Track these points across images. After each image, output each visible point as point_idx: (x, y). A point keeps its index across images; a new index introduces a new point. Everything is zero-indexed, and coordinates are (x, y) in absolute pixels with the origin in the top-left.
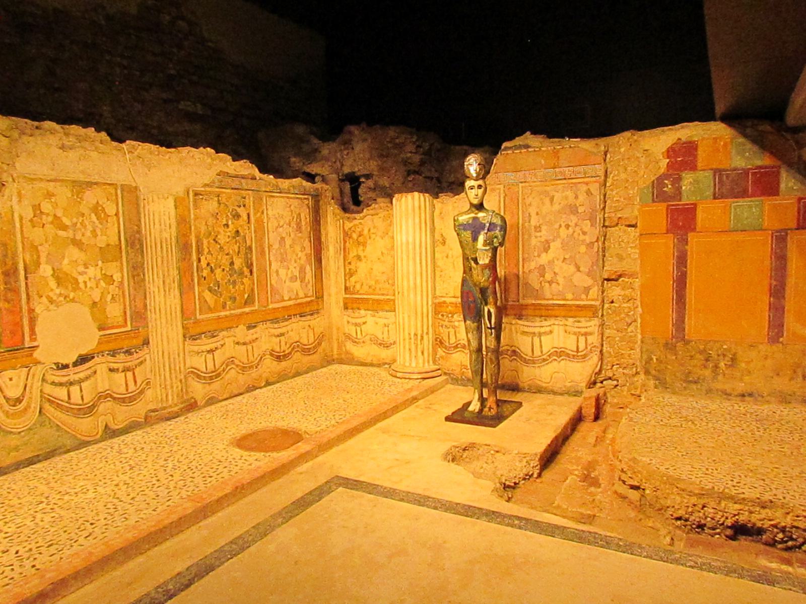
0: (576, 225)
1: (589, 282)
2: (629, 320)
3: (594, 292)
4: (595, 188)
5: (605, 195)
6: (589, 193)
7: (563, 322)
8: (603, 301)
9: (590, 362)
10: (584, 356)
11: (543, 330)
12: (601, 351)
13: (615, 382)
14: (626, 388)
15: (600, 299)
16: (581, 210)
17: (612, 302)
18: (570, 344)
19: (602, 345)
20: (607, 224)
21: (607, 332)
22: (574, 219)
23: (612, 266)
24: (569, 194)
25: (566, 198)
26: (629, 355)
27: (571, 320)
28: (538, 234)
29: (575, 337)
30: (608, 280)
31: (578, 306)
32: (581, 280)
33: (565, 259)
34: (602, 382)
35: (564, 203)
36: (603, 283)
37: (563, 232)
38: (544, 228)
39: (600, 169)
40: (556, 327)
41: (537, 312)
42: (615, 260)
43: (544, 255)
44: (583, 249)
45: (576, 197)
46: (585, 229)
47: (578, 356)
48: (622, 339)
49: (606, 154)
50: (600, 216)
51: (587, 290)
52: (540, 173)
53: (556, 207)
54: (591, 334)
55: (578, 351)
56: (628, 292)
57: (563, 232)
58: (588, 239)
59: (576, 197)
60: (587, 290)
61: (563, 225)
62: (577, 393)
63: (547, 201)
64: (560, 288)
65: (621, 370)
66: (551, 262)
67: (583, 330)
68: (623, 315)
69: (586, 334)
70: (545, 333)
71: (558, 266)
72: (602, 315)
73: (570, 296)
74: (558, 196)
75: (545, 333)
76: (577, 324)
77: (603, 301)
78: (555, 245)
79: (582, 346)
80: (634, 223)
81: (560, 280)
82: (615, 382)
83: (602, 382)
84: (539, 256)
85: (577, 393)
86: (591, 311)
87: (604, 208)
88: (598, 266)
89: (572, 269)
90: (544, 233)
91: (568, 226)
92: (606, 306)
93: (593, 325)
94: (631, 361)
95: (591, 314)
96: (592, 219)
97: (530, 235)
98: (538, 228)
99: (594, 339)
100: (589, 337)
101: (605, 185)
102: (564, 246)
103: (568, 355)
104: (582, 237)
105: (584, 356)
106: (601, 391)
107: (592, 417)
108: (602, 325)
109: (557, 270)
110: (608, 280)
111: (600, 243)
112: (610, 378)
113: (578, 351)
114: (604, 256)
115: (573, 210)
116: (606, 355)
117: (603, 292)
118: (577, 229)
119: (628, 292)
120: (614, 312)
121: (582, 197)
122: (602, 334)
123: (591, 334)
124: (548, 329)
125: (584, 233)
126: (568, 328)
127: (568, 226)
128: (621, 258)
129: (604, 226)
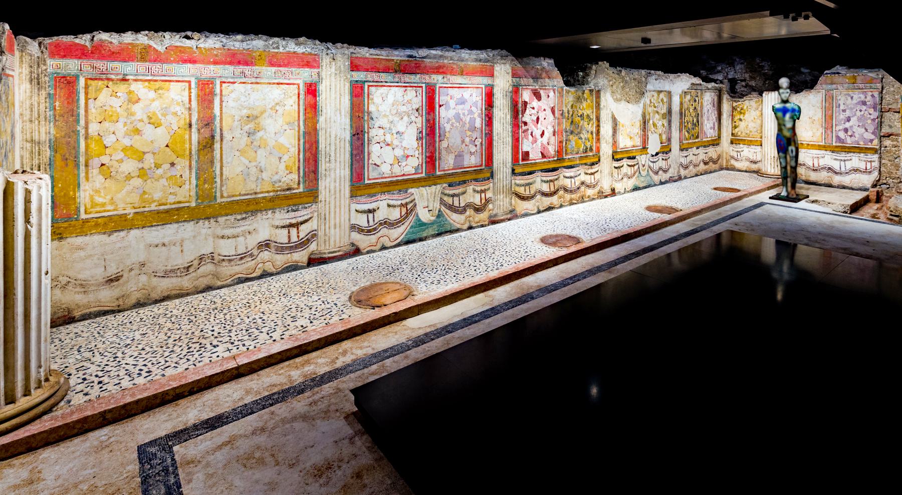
0: (866, 110)
1: (873, 137)
2: (896, 156)
3: (876, 142)
4: (876, 94)
5: (882, 98)
6: (873, 96)
7: (858, 155)
8: (881, 146)
9: (874, 175)
10: (870, 172)
11: (846, 158)
12: (880, 170)
13: (888, 186)
14: (894, 189)
15: (879, 145)
16: (868, 103)
17: (886, 147)
18: (862, 166)
19: (880, 167)
20: (883, 110)
21: (883, 161)
22: (864, 108)
23: (885, 130)
24: (862, 97)
25: (860, 98)
26: (896, 173)
27: (862, 154)
28: (844, 113)
29: (865, 163)
30: (884, 136)
31: (866, 148)
32: (869, 136)
33: (859, 126)
34: (880, 185)
35: (859, 100)
36: (880, 138)
37: (858, 113)
38: (847, 111)
39: (879, 86)
40: (853, 158)
41: (843, 150)
42: (887, 127)
43: (847, 123)
44: (869, 121)
45: (866, 98)
46: (871, 113)
47: (866, 172)
48: (891, 165)
49: (882, 79)
50: (879, 107)
51: (871, 141)
52: (846, 86)
53: (855, 101)
54: (874, 161)
55: (866, 169)
56: (895, 143)
57: (858, 113)
58: (872, 117)
59: (866, 98)
60: (871, 141)
61: (858, 110)
62: (866, 190)
63: (849, 98)
64: (857, 139)
65: (891, 180)
66: (851, 127)
67: (869, 160)
68: (892, 154)
69: (871, 162)
70: (848, 160)
71: (855, 129)
72: (880, 153)
73: (862, 143)
74: (855, 97)
75: (848, 160)
76: (866, 157)
77: (881, 146)
78: (854, 120)
79: (869, 167)
80: (898, 111)
81: (857, 135)
82: (888, 186)
83: (880, 185)
84: (844, 123)
85: (866, 190)
86: (875, 151)
87: (881, 103)
88: (877, 129)
89: (863, 130)
90: (848, 113)
91: (861, 111)
92: (883, 149)
93: (876, 157)
94: (897, 176)
95: (874, 152)
96: (875, 108)
97: (840, 114)
98: (844, 111)
99: (876, 164)
100: (872, 163)
101: (882, 93)
102: (859, 120)
103: (861, 171)
104: (869, 116)
105: (870, 172)
106: (880, 189)
107: (875, 201)
108: (880, 158)
109: (854, 131)
110: (884, 136)
111: (879, 119)
112: (885, 184)
113: (866, 169)
114: (881, 125)
115: (864, 103)
116: (882, 172)
117: (881, 142)
118: (866, 112)
119: (895, 143)
120: (887, 152)
121: (869, 98)
122: (880, 162)
123: (874, 161)
124: (849, 158)
125: (870, 114)
126: (861, 158)
127: (861, 111)
128: (890, 127)
129: (881, 111)
